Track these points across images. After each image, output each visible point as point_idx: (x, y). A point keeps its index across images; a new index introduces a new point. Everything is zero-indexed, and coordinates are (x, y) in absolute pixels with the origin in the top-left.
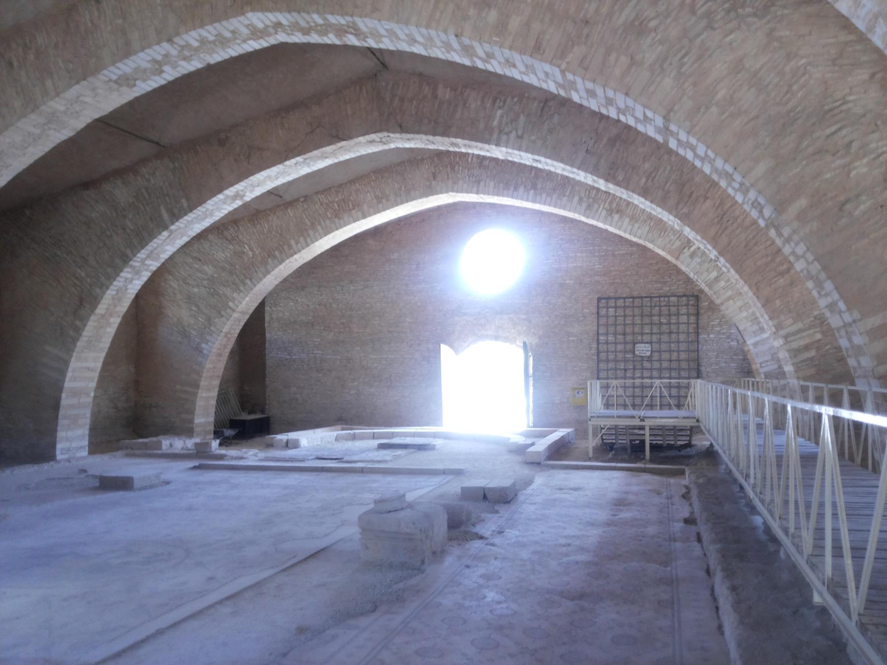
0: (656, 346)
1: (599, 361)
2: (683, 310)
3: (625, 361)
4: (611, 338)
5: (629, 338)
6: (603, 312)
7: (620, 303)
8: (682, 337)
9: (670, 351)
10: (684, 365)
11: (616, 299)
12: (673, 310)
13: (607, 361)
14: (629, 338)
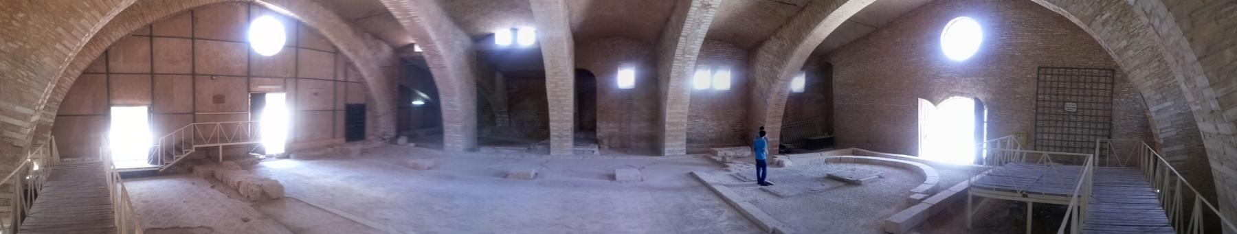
0: (1081, 105)
1: (1037, 114)
2: (1103, 80)
3: (1057, 114)
4: (1047, 97)
5: (1061, 98)
6: (1042, 77)
7: (1056, 71)
8: (1100, 99)
9: (1091, 109)
10: (1100, 120)
11: (1053, 68)
12: (1095, 79)
13: (1044, 114)
14: (1061, 98)
